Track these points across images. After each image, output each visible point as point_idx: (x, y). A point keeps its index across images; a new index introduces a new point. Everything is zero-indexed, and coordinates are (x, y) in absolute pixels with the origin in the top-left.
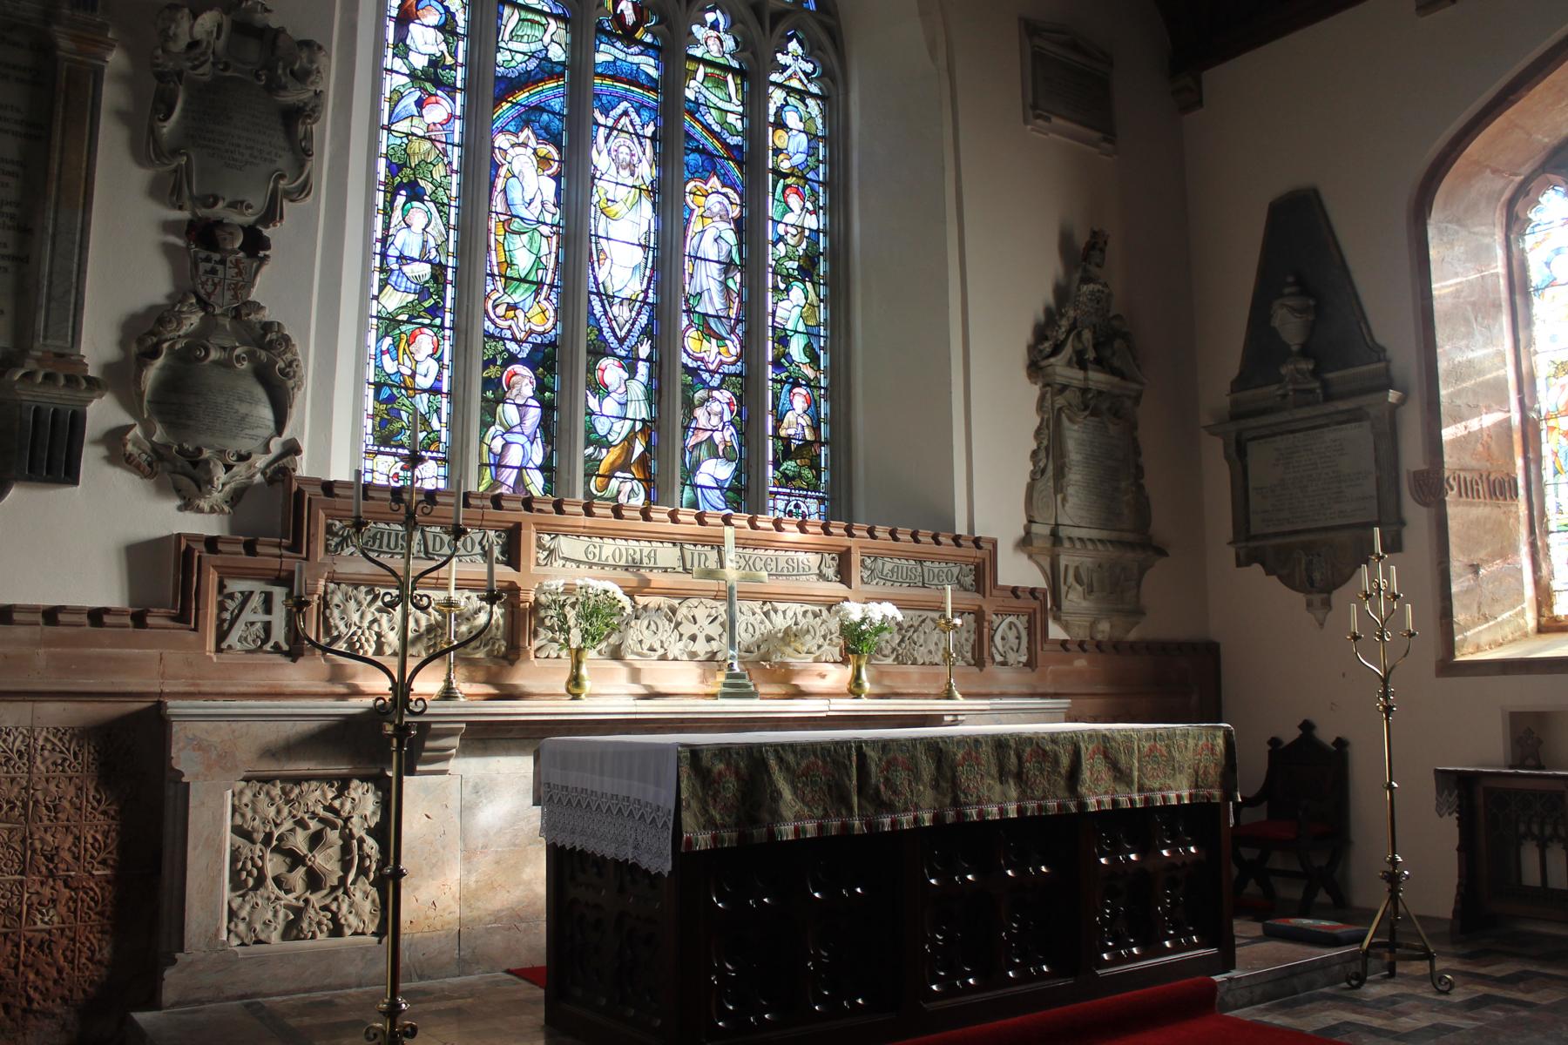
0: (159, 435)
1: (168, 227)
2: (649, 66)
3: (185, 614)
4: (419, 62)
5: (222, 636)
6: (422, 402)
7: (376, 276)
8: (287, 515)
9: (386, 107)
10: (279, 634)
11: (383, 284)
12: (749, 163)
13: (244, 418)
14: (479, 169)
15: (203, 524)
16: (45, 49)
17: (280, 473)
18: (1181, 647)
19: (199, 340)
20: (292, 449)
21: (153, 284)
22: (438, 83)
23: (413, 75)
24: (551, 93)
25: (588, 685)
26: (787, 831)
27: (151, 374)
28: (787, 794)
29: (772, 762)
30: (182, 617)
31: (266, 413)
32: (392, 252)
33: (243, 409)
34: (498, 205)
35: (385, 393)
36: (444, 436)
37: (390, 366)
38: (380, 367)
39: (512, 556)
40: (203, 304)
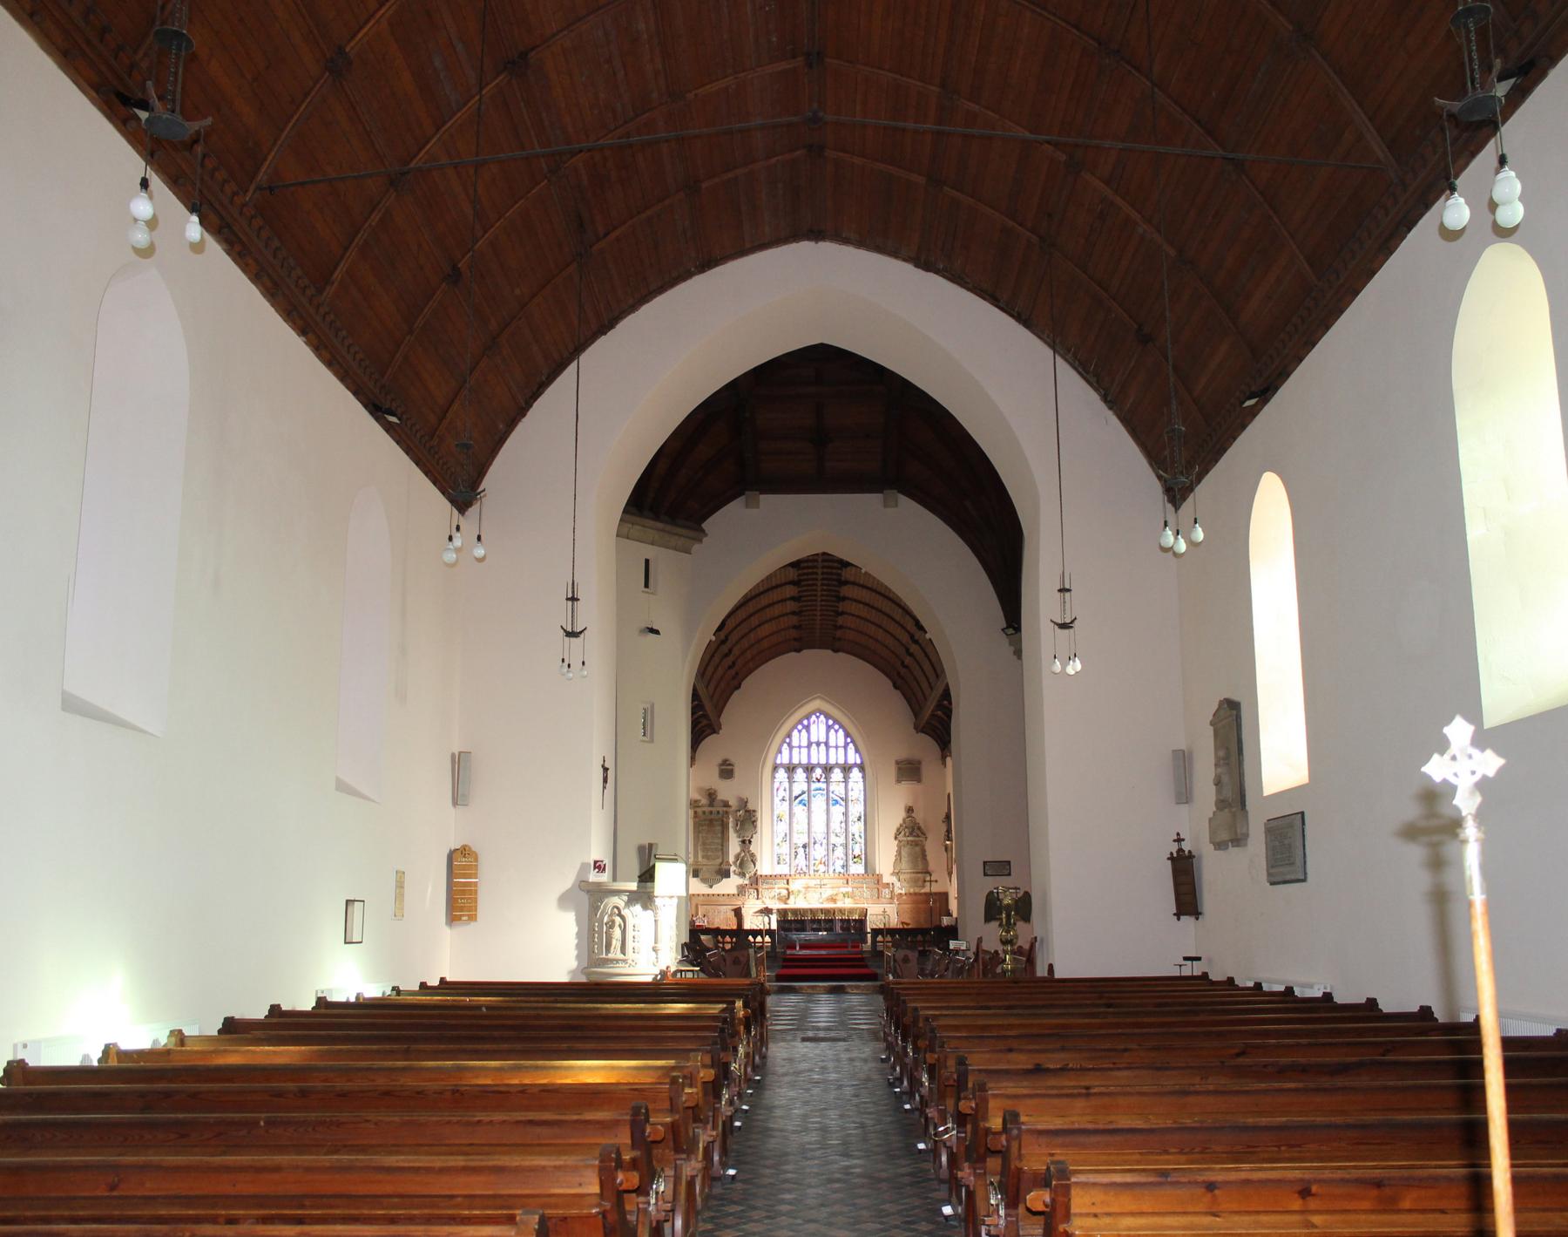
2: (824, 786)
8: (756, 881)
12: (846, 800)
21: (738, 849)
24: (805, 797)
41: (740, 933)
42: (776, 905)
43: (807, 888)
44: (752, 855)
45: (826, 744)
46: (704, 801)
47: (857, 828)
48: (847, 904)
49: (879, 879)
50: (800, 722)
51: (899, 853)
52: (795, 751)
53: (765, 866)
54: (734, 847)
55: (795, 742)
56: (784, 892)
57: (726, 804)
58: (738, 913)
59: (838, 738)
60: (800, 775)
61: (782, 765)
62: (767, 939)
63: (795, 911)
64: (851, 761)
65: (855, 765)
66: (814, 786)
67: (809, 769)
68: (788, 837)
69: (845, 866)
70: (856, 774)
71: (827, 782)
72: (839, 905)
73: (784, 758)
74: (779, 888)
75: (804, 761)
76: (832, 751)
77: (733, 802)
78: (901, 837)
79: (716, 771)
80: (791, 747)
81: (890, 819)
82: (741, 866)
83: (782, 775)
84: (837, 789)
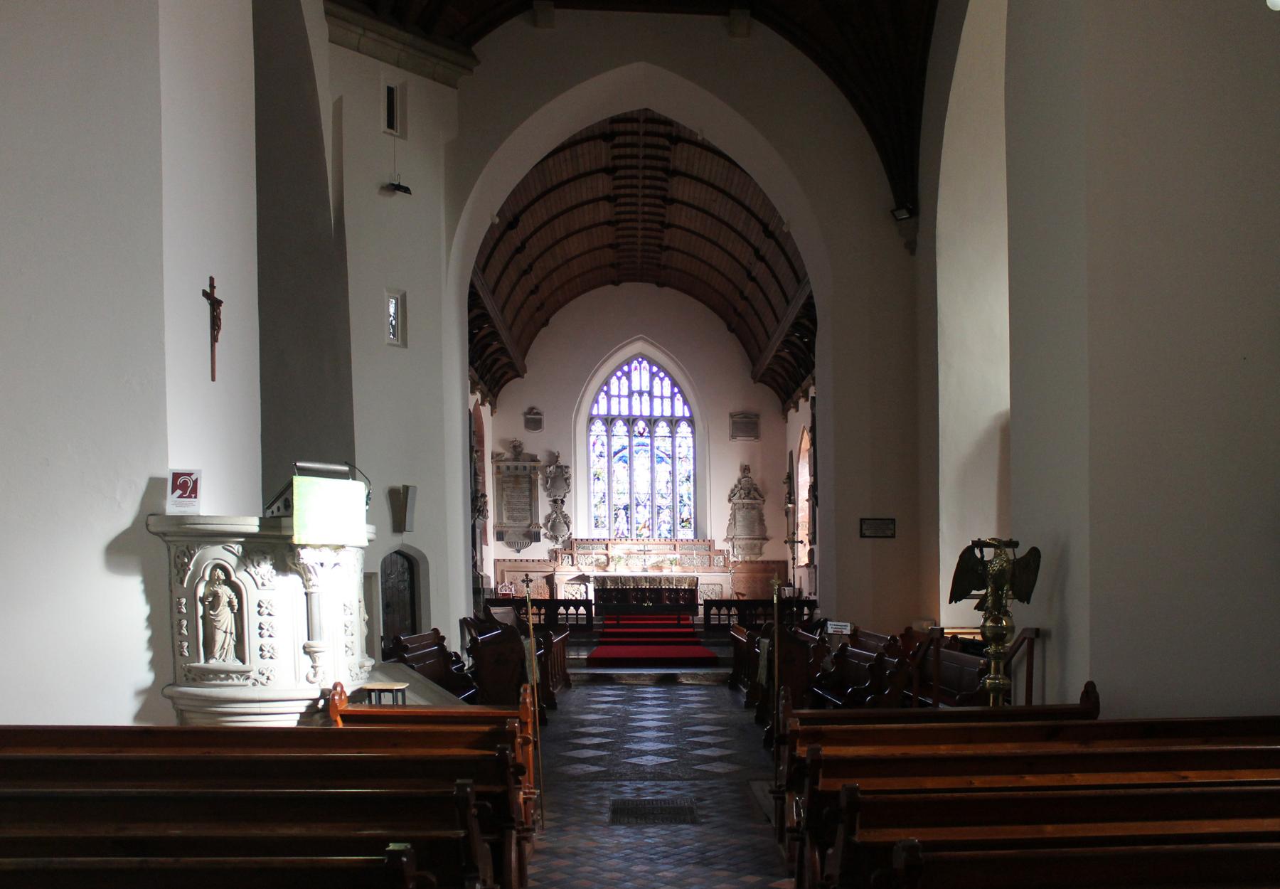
2: (648, 441)
8: (570, 545)
14: (610, 473)
15: (559, 546)
18: (778, 562)
21: (549, 511)
34: (614, 479)
41: (552, 604)
42: (593, 572)
43: (629, 554)
44: (566, 517)
45: (650, 393)
46: (508, 455)
47: (686, 489)
48: (675, 572)
49: (710, 545)
50: (619, 368)
51: (733, 517)
52: (614, 401)
53: (580, 529)
54: (544, 507)
55: (614, 391)
56: (603, 559)
58: (550, 580)
59: (663, 387)
60: (620, 428)
61: (599, 416)
62: (582, 610)
63: (615, 579)
64: (679, 413)
65: (683, 418)
66: (636, 441)
67: (630, 421)
68: (607, 496)
69: (672, 531)
70: (684, 429)
71: (652, 436)
72: (666, 573)
73: (601, 408)
74: (598, 553)
75: (625, 412)
76: (657, 402)
77: (542, 457)
78: (735, 499)
79: (521, 420)
80: (609, 396)
81: (724, 479)
82: (553, 528)
83: (598, 427)
84: (663, 445)
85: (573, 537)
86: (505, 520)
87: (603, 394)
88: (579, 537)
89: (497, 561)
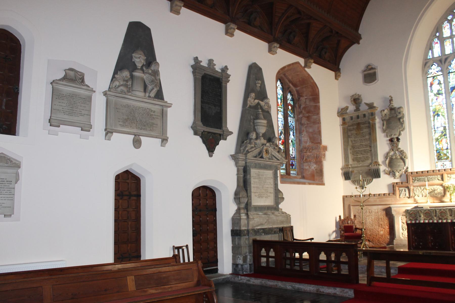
0: (390, 169)
1: (387, 141)
3: (394, 193)
4: (435, 92)
5: (400, 196)
6: (445, 152)
7: (434, 132)
9: (430, 102)
10: (408, 195)
11: (435, 133)
13: (399, 165)
16: (369, 123)
17: (406, 171)
19: (392, 156)
20: (407, 168)
22: (439, 94)
23: (435, 95)
25: (452, 200)
26: (422, 221)
27: (387, 162)
28: (422, 216)
29: (420, 212)
30: (394, 194)
31: (403, 163)
32: (436, 127)
33: (399, 164)
35: (438, 152)
36: (450, 157)
37: (438, 147)
38: (436, 147)
39: (442, 179)
40: (393, 150)
44: (402, 152)
56: (440, 189)
57: (371, 106)
73: (437, 51)
74: (435, 185)
79: (360, 77)
80: (442, 40)
83: (435, 69)
85: (410, 170)
86: (351, 162)
87: (436, 40)
88: (416, 170)
89: (345, 198)
